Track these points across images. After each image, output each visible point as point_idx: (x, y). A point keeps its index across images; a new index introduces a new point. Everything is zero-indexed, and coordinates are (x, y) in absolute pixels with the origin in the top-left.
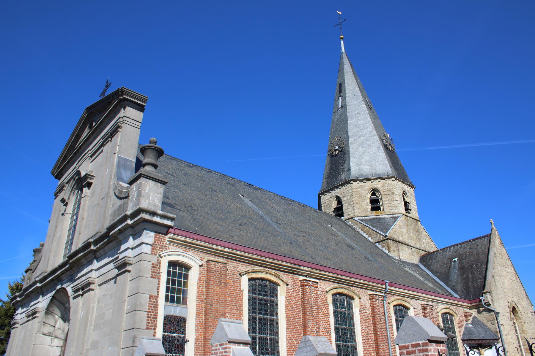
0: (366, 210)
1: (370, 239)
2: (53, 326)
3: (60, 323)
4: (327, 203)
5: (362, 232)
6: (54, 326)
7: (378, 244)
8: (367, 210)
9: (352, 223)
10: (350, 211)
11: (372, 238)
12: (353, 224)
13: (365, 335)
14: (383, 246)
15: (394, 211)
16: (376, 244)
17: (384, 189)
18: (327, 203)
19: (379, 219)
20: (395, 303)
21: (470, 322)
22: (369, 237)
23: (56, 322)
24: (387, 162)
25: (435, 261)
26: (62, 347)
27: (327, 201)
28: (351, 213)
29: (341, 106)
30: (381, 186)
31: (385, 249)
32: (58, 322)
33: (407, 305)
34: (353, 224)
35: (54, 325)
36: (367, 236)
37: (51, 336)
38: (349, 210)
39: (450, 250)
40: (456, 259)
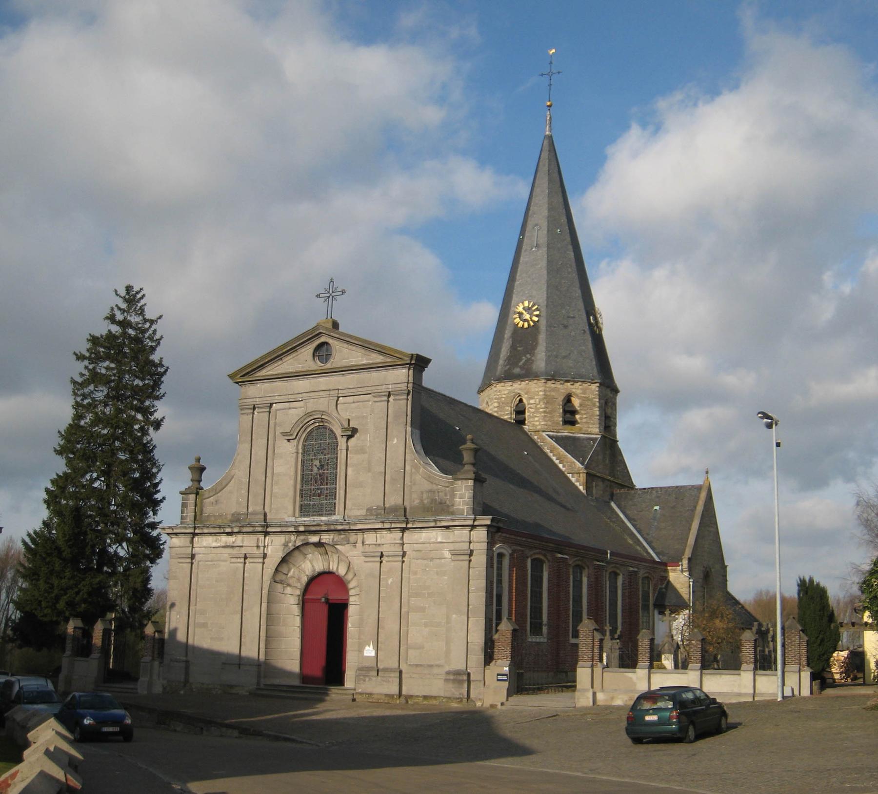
0: (557, 423)
1: (561, 466)
2: (286, 574)
3: (294, 572)
4: (503, 399)
5: (551, 454)
6: (287, 574)
7: (571, 475)
8: (559, 424)
9: (538, 438)
10: (537, 421)
11: (563, 466)
12: (539, 440)
13: (589, 602)
14: (577, 481)
15: (592, 429)
16: (568, 475)
17: (583, 397)
18: (503, 399)
19: (574, 439)
20: (610, 571)
21: (663, 586)
22: (560, 463)
23: (289, 570)
24: (593, 356)
25: (630, 502)
26: (299, 596)
27: (504, 396)
28: (537, 423)
29: (537, 244)
30: (581, 391)
31: (580, 485)
32: (293, 570)
33: (618, 571)
34: (539, 440)
35: (286, 573)
36: (557, 462)
37: (283, 584)
38: (536, 419)
39: (651, 492)
40: (657, 508)
